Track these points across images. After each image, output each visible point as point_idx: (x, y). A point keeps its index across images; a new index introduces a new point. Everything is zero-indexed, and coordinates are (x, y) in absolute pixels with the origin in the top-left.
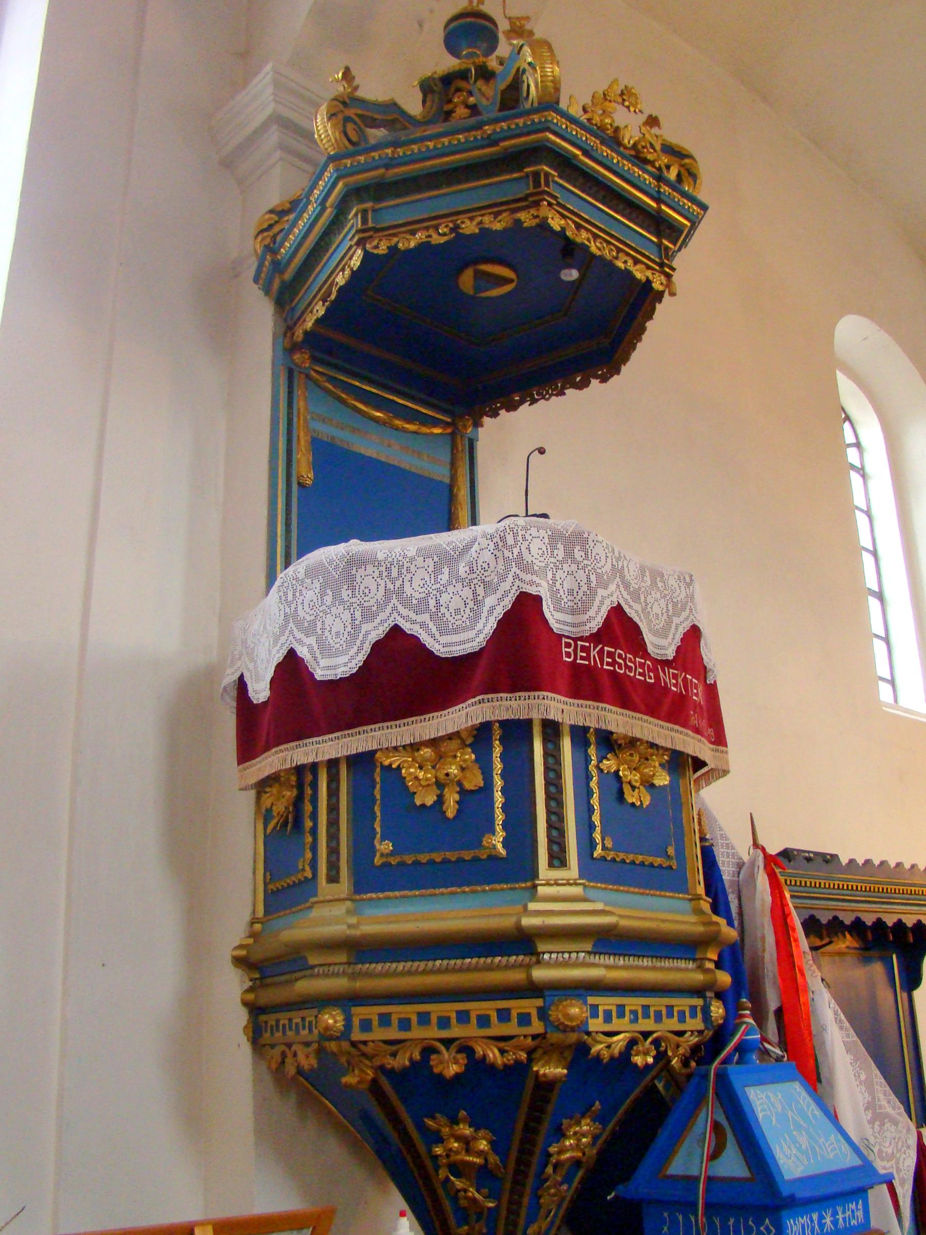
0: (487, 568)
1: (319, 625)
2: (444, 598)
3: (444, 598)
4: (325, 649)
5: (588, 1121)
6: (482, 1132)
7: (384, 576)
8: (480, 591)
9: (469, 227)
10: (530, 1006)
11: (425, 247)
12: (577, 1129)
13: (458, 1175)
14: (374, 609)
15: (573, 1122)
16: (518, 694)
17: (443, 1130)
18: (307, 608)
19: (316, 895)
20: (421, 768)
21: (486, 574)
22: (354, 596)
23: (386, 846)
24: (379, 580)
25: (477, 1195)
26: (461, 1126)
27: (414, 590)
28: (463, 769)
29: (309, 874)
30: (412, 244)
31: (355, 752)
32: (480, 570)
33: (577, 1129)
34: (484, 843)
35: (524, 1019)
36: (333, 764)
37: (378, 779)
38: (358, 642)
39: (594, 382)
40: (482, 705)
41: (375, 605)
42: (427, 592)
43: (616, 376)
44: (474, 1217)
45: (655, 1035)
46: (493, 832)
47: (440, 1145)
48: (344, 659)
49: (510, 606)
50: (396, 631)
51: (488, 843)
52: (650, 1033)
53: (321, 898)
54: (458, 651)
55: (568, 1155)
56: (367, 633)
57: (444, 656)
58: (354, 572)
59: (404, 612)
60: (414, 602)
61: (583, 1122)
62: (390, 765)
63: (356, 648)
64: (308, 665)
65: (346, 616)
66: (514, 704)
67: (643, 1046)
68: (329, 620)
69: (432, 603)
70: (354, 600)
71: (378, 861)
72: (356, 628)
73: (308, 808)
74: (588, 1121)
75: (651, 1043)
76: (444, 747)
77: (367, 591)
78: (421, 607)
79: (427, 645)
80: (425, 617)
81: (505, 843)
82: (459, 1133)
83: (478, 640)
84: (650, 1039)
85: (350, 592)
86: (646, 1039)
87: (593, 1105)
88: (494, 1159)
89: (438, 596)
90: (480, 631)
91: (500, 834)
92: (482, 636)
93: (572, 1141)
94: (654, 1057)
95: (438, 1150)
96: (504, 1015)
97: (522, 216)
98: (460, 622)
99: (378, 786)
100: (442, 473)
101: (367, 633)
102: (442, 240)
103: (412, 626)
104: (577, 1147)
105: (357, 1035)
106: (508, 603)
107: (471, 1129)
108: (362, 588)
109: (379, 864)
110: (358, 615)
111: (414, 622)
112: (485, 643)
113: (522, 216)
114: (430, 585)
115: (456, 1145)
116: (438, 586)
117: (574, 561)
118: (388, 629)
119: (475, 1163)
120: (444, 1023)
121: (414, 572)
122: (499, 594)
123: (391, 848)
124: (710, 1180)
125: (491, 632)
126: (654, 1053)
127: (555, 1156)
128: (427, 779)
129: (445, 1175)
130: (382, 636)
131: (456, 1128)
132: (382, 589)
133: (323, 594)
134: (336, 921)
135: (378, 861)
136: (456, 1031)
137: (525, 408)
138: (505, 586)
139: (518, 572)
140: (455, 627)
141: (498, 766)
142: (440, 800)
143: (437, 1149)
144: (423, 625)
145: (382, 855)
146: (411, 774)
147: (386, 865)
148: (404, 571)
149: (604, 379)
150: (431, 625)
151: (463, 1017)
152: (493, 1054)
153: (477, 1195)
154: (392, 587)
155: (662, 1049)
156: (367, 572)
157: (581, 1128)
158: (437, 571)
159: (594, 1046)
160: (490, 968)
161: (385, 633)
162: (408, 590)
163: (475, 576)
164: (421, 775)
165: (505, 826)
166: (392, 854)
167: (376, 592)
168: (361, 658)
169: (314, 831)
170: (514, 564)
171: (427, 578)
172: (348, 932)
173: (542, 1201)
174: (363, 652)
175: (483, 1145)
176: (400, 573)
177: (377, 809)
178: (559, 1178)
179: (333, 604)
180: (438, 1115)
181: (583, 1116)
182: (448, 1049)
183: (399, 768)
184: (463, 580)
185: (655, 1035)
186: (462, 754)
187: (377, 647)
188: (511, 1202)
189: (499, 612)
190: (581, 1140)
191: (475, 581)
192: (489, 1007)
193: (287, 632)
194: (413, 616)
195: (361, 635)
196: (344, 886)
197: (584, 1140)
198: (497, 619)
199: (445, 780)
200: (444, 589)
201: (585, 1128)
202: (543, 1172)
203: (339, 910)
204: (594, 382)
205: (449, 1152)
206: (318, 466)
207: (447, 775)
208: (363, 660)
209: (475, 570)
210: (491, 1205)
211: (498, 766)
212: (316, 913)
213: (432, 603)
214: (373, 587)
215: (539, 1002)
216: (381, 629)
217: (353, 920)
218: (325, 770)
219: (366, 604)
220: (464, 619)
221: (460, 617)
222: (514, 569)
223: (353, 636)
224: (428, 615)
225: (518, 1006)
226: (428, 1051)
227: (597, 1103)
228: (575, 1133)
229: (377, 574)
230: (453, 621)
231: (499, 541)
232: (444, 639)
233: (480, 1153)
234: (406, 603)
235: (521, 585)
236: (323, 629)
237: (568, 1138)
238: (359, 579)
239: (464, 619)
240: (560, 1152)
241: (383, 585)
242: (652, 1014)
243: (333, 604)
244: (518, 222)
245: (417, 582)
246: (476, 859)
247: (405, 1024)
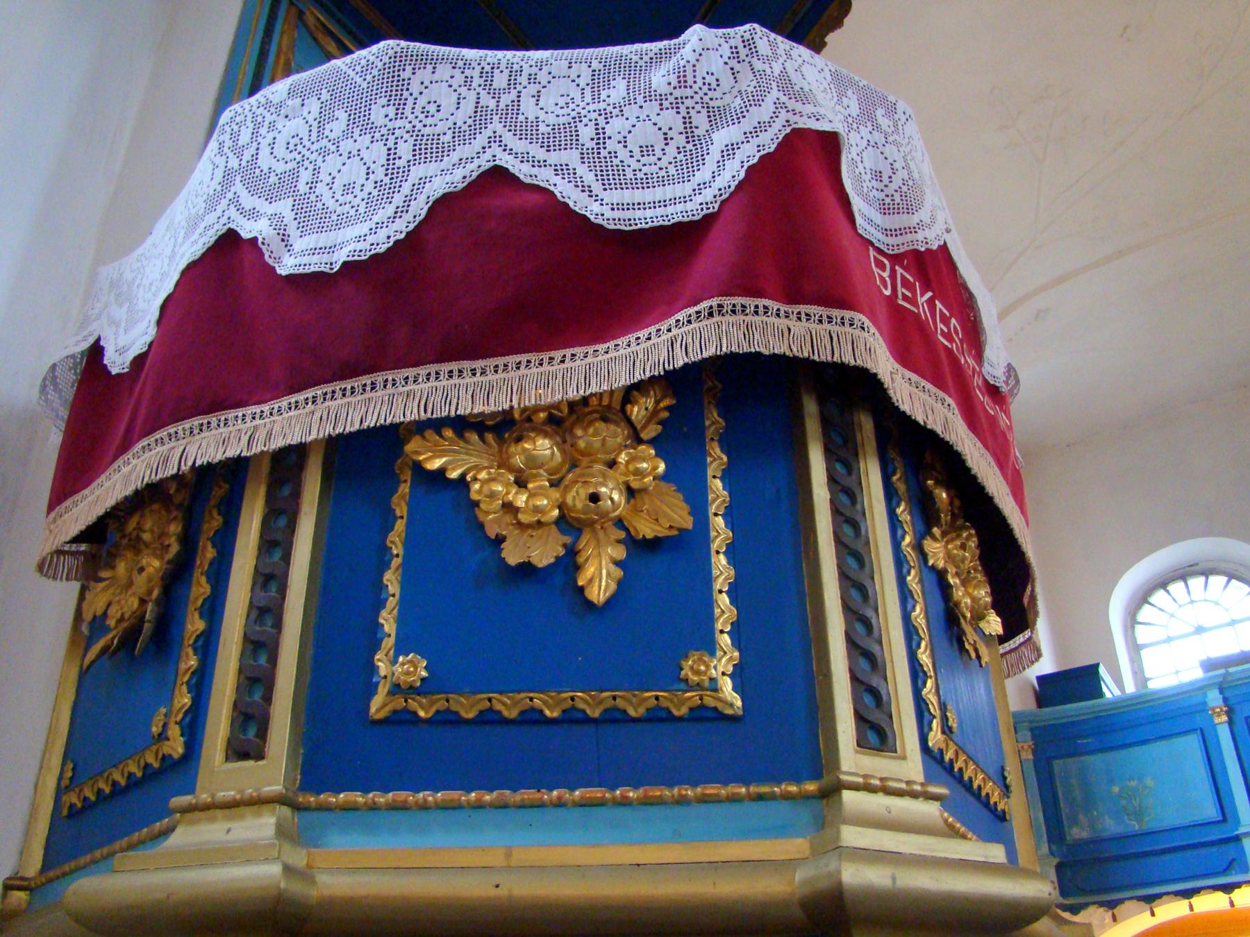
0: (714, 85)
1: (305, 176)
2: (616, 126)
3: (616, 126)
7: (475, 85)
8: (701, 120)
14: (448, 138)
16: (803, 308)
18: (280, 150)
19: (191, 790)
20: (521, 483)
21: (711, 94)
22: (399, 115)
23: (412, 668)
24: (463, 90)
28: (631, 492)
29: (176, 746)
31: (356, 427)
32: (700, 83)
34: (686, 672)
37: (401, 509)
38: (398, 199)
40: (717, 318)
41: (450, 133)
42: (573, 114)
46: (710, 647)
48: (363, 229)
49: (773, 147)
51: (697, 673)
53: (205, 797)
56: (423, 181)
57: (612, 227)
58: (407, 74)
59: (520, 146)
60: (542, 128)
62: (442, 471)
63: (390, 210)
64: (264, 248)
65: (378, 153)
66: (799, 328)
69: (586, 133)
70: (399, 123)
71: (378, 705)
72: (395, 173)
73: (200, 588)
76: (591, 437)
77: (432, 108)
78: (562, 137)
79: (571, 204)
80: (571, 157)
81: (739, 675)
83: (699, 199)
85: (391, 111)
89: (601, 121)
90: (704, 185)
92: (708, 194)
98: (654, 169)
99: (400, 526)
101: (423, 181)
103: (535, 171)
106: (769, 141)
108: (422, 101)
109: (381, 715)
110: (405, 150)
111: (543, 164)
112: (717, 206)
114: (582, 105)
116: (602, 106)
117: (876, 127)
118: (475, 175)
121: (544, 83)
122: (747, 124)
123: (424, 674)
125: (734, 184)
128: (537, 510)
130: (461, 186)
132: (468, 107)
133: (325, 117)
134: (247, 853)
135: (378, 705)
139: (784, 99)
140: (640, 175)
142: (570, 562)
144: (559, 170)
145: (396, 689)
146: (492, 495)
147: (401, 719)
148: (523, 80)
150: (582, 170)
154: (492, 104)
156: (436, 77)
161: (468, 180)
162: (529, 109)
163: (689, 92)
164: (521, 500)
165: (737, 633)
166: (424, 689)
167: (453, 109)
168: (401, 228)
169: (207, 645)
170: (774, 85)
171: (576, 94)
172: (282, 885)
174: (408, 217)
176: (512, 83)
177: (392, 581)
179: (347, 134)
183: (462, 482)
184: (661, 98)
186: (632, 459)
187: (444, 205)
189: (750, 154)
191: (689, 103)
193: (224, 202)
194: (541, 154)
195: (406, 188)
198: (746, 165)
199: (585, 510)
200: (616, 112)
203: (263, 826)
207: (595, 498)
208: (405, 230)
209: (690, 82)
212: (184, 836)
213: (586, 133)
214: (448, 101)
216: (459, 174)
217: (298, 858)
218: (262, 491)
219: (426, 131)
220: (663, 163)
221: (652, 159)
222: (775, 93)
223: (386, 191)
224: (575, 154)
229: (459, 80)
230: (635, 165)
231: (741, 45)
232: (614, 196)
234: (527, 131)
235: (793, 119)
236: (312, 185)
238: (415, 88)
239: (663, 163)
241: (472, 96)
243: (347, 134)
245: (548, 100)
246: (659, 716)
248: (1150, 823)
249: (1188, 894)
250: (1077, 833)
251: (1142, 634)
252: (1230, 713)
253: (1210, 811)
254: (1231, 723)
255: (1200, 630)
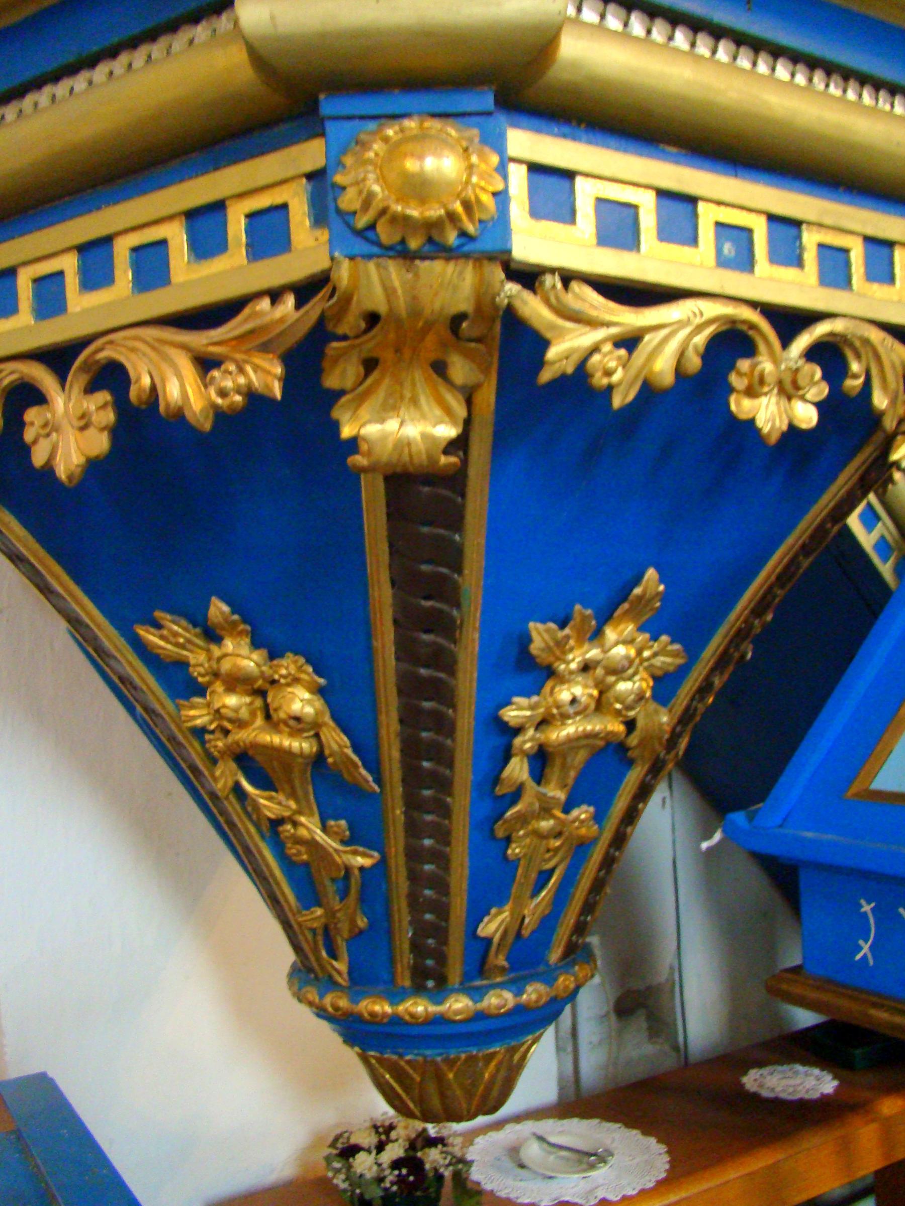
5: (629, 628)
6: (284, 662)
12: (594, 653)
13: (264, 782)
15: (567, 631)
17: (192, 658)
25: (320, 836)
26: (229, 645)
33: (594, 653)
44: (330, 889)
45: (821, 329)
47: (197, 700)
52: (808, 318)
55: (570, 729)
61: (611, 634)
67: (776, 362)
74: (629, 628)
75: (813, 353)
82: (226, 666)
84: (803, 341)
86: (787, 334)
87: (637, 580)
93: (578, 691)
94: (820, 406)
104: (600, 705)
107: (256, 656)
115: (232, 700)
119: (289, 753)
126: (820, 391)
127: (531, 732)
129: (230, 783)
131: (216, 651)
143: (192, 713)
153: (320, 836)
155: (853, 384)
157: (605, 651)
159: (561, 333)
173: (514, 850)
178: (556, 792)
180: (158, 614)
181: (605, 617)
182: (62, 376)
185: (821, 329)
188: (413, 855)
190: (612, 686)
197: (623, 686)
201: (620, 651)
202: (496, 780)
210: (360, 861)
227: (651, 574)
228: (586, 668)
233: (297, 725)
237: (562, 680)
240: (544, 723)
242: (810, 256)
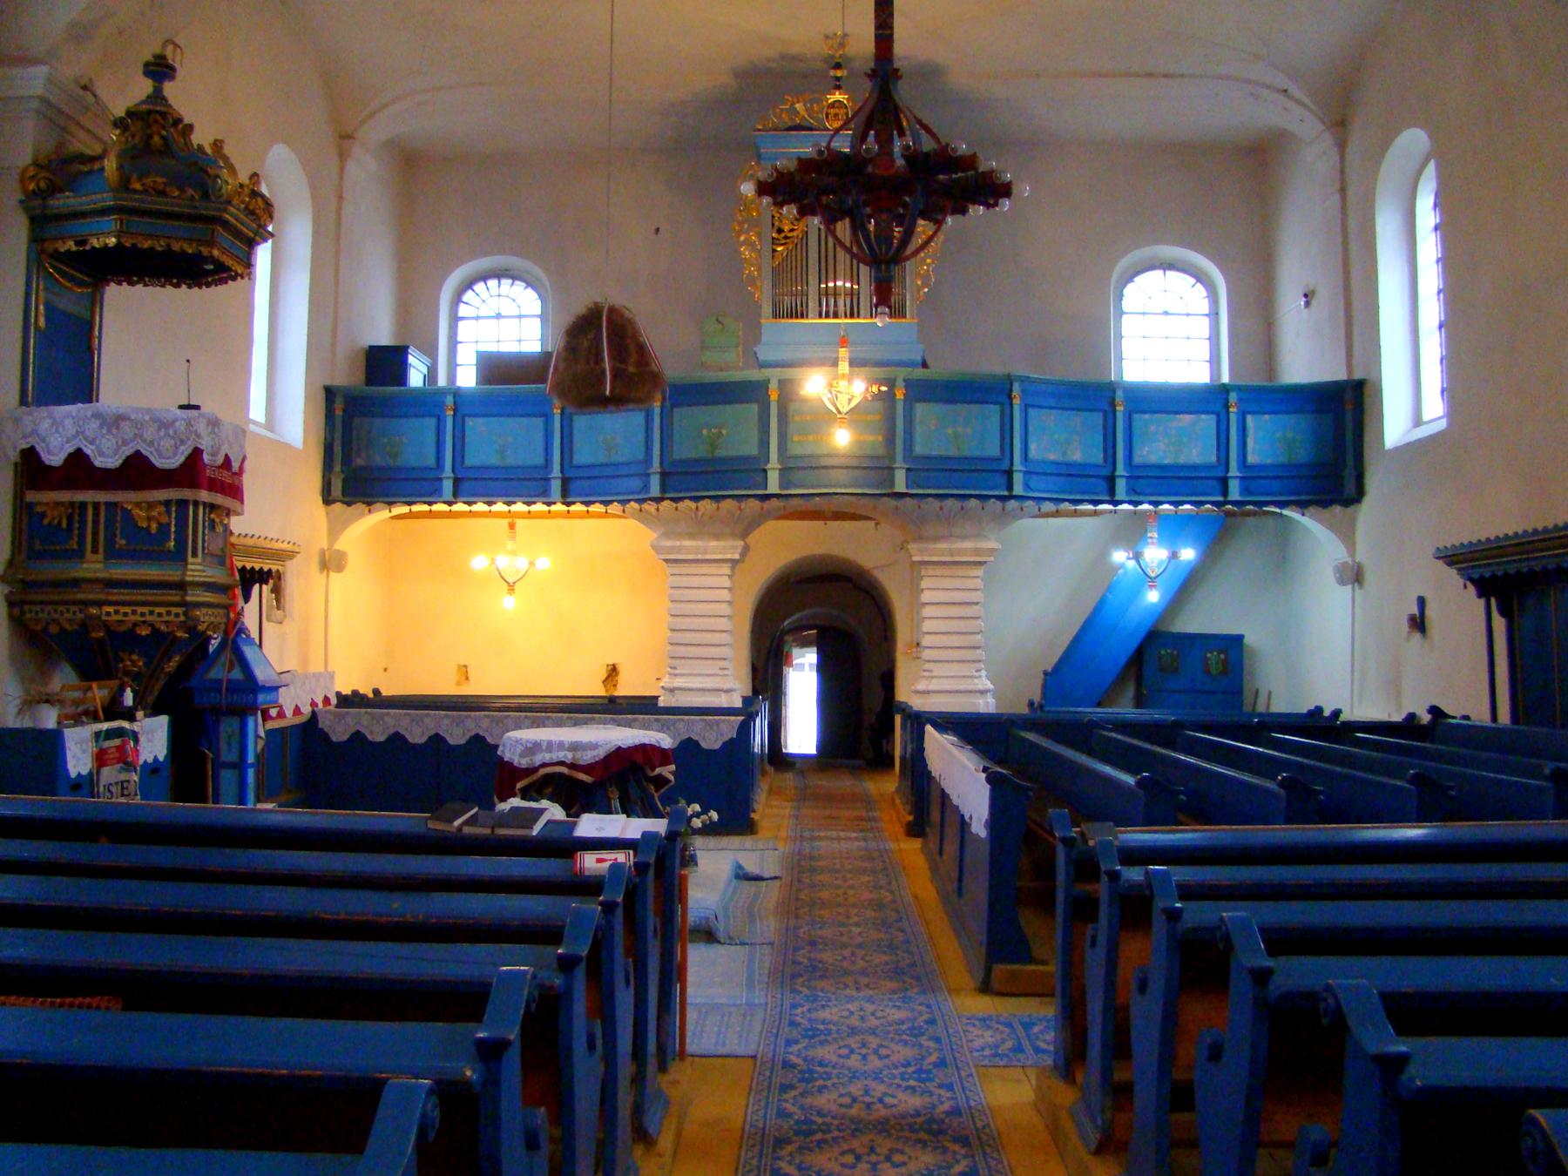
3: (162, 443)
4: (101, 454)
9: (176, 247)
10: (180, 610)
11: (152, 249)
27: (148, 436)
30: (146, 246)
35: (177, 615)
36: (96, 505)
39: (184, 286)
43: (197, 288)
50: (138, 453)
54: (166, 466)
65: (114, 441)
68: (104, 441)
69: (156, 444)
78: (151, 444)
80: (152, 449)
88: (144, 669)
91: (172, 544)
95: (121, 665)
96: (169, 613)
97: (202, 249)
100: (87, 315)
102: (160, 249)
105: (104, 618)
110: (120, 442)
113: (202, 249)
120: (143, 614)
124: (229, 681)
136: (149, 618)
137: (140, 286)
138: (189, 443)
141: (174, 515)
144: (151, 453)
149: (190, 287)
151: (151, 613)
152: (163, 628)
158: (159, 429)
160: (163, 595)
162: (145, 435)
175: (141, 663)
192: (163, 610)
196: (100, 557)
204: (184, 286)
205: (126, 666)
206: (48, 320)
211: (174, 515)
212: (85, 566)
215: (184, 609)
225: (174, 610)
226: (136, 624)
233: (140, 667)
244: (200, 252)
245: (149, 433)
247: (125, 614)
248: (399, 463)
249: (410, 504)
250: (360, 462)
251: (463, 310)
252: (455, 410)
253: (431, 461)
254: (454, 416)
255: (499, 316)
